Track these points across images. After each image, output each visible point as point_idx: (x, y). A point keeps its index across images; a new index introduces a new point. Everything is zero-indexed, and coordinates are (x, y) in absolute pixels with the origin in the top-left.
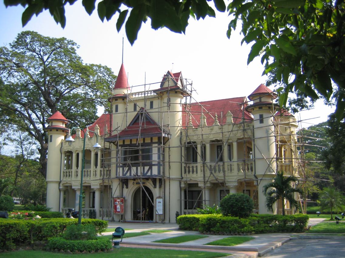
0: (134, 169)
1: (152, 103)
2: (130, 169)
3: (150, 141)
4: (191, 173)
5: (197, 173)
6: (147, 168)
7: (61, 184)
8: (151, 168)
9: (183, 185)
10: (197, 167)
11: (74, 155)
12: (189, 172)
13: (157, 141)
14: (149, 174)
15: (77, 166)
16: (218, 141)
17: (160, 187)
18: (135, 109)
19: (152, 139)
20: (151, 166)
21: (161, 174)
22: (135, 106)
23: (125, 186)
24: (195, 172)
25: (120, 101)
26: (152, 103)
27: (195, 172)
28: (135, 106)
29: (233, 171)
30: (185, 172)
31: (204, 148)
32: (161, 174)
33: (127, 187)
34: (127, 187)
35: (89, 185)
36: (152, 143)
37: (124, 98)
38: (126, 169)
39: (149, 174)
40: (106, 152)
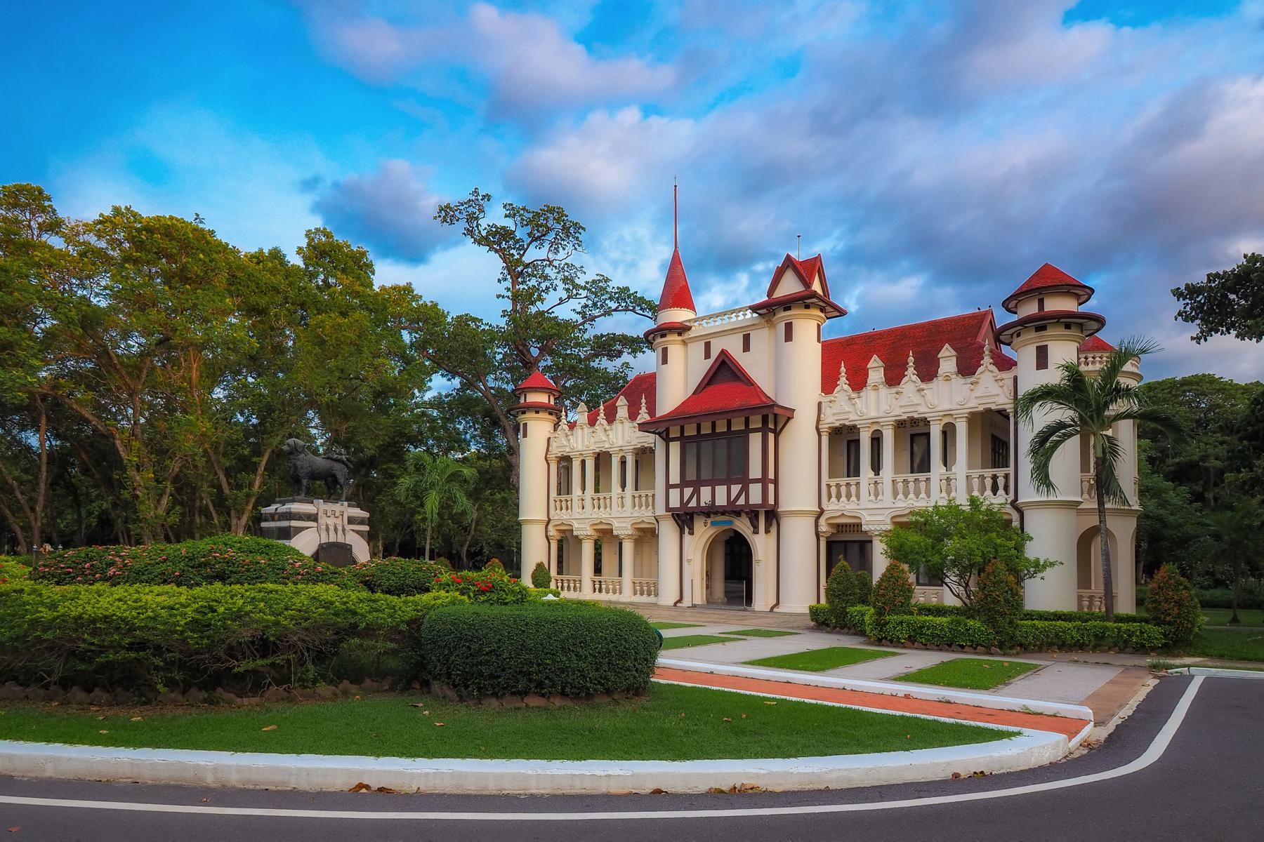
0: (706, 492)
1: (747, 339)
2: (697, 492)
4: (843, 499)
6: (736, 489)
8: (745, 490)
9: (824, 527)
10: (858, 484)
11: (576, 466)
12: (839, 497)
14: (741, 501)
15: (584, 489)
17: (767, 531)
18: (707, 356)
20: (746, 482)
21: (771, 501)
22: (708, 345)
23: (687, 530)
24: (853, 498)
25: (673, 337)
26: (747, 339)
28: (708, 345)
30: (830, 497)
32: (771, 501)
33: (691, 533)
34: (691, 533)
36: (748, 430)
38: (688, 491)
39: (741, 501)
40: (644, 456)
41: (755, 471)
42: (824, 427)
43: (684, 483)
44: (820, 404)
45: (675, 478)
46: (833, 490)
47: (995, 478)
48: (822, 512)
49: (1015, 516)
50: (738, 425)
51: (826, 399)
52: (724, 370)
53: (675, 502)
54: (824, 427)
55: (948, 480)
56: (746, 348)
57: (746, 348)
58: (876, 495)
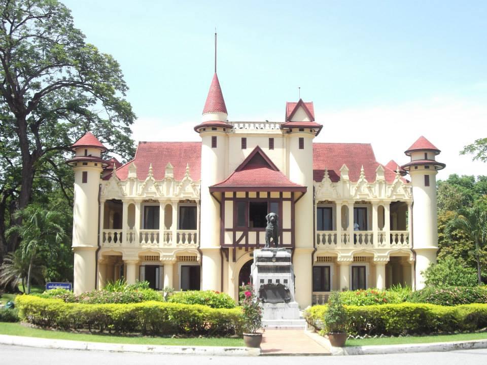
2: (246, 235)
3: (278, 196)
5: (335, 242)
7: (100, 253)
13: (289, 196)
16: (364, 202)
18: (244, 146)
19: (281, 194)
22: (244, 141)
27: (333, 243)
28: (244, 141)
29: (384, 243)
31: (345, 209)
35: (156, 255)
37: (227, 127)
38: (239, 234)
41: (287, 224)
42: (317, 202)
43: (234, 230)
44: (314, 188)
45: (229, 223)
46: (321, 238)
47: (397, 235)
48: (316, 250)
49: (412, 255)
50: (275, 195)
51: (317, 184)
52: (257, 160)
53: (228, 240)
54: (317, 202)
55: (382, 235)
56: (271, 146)
57: (271, 146)
58: (345, 241)
